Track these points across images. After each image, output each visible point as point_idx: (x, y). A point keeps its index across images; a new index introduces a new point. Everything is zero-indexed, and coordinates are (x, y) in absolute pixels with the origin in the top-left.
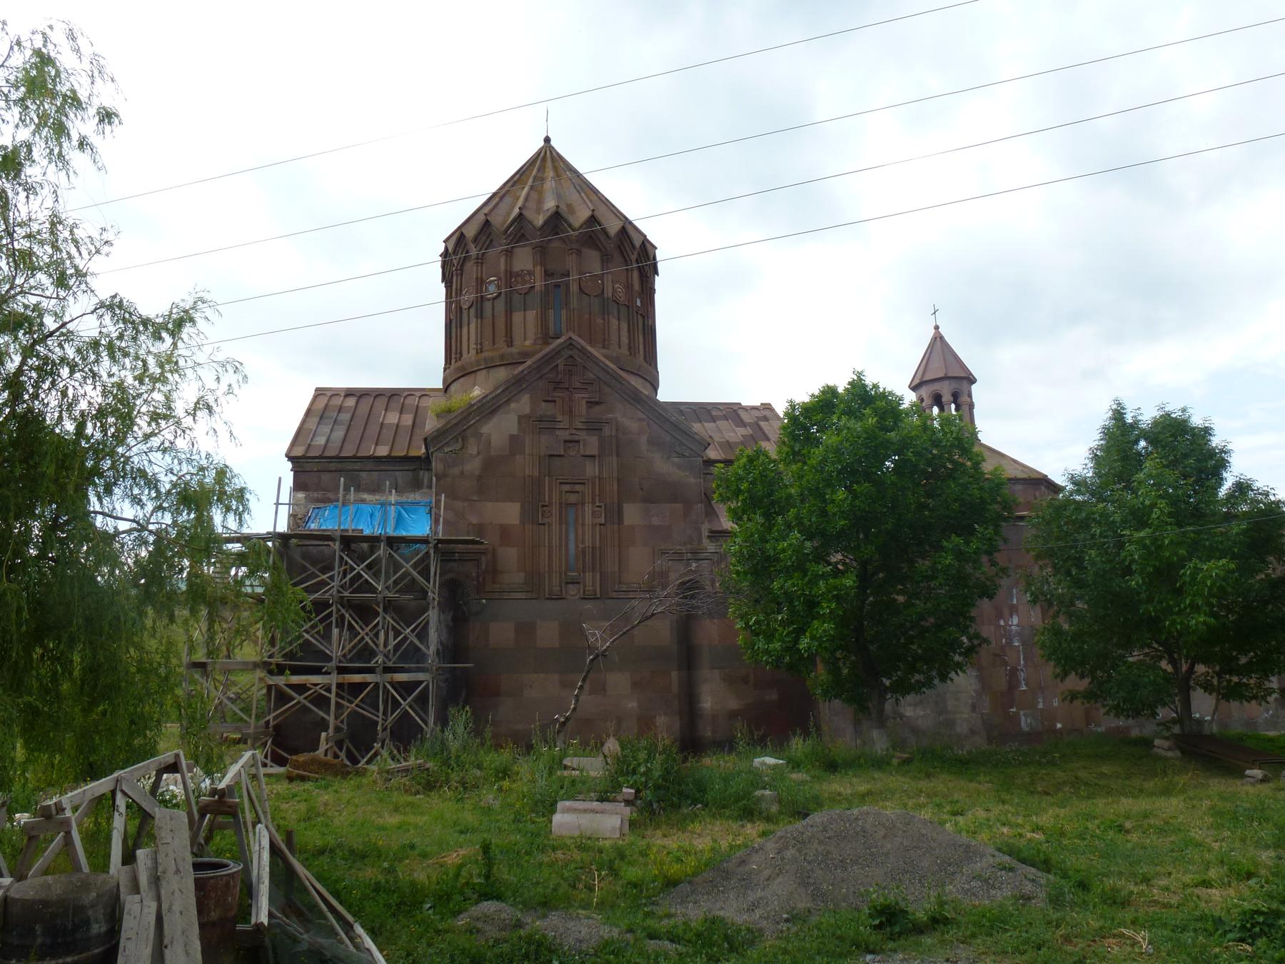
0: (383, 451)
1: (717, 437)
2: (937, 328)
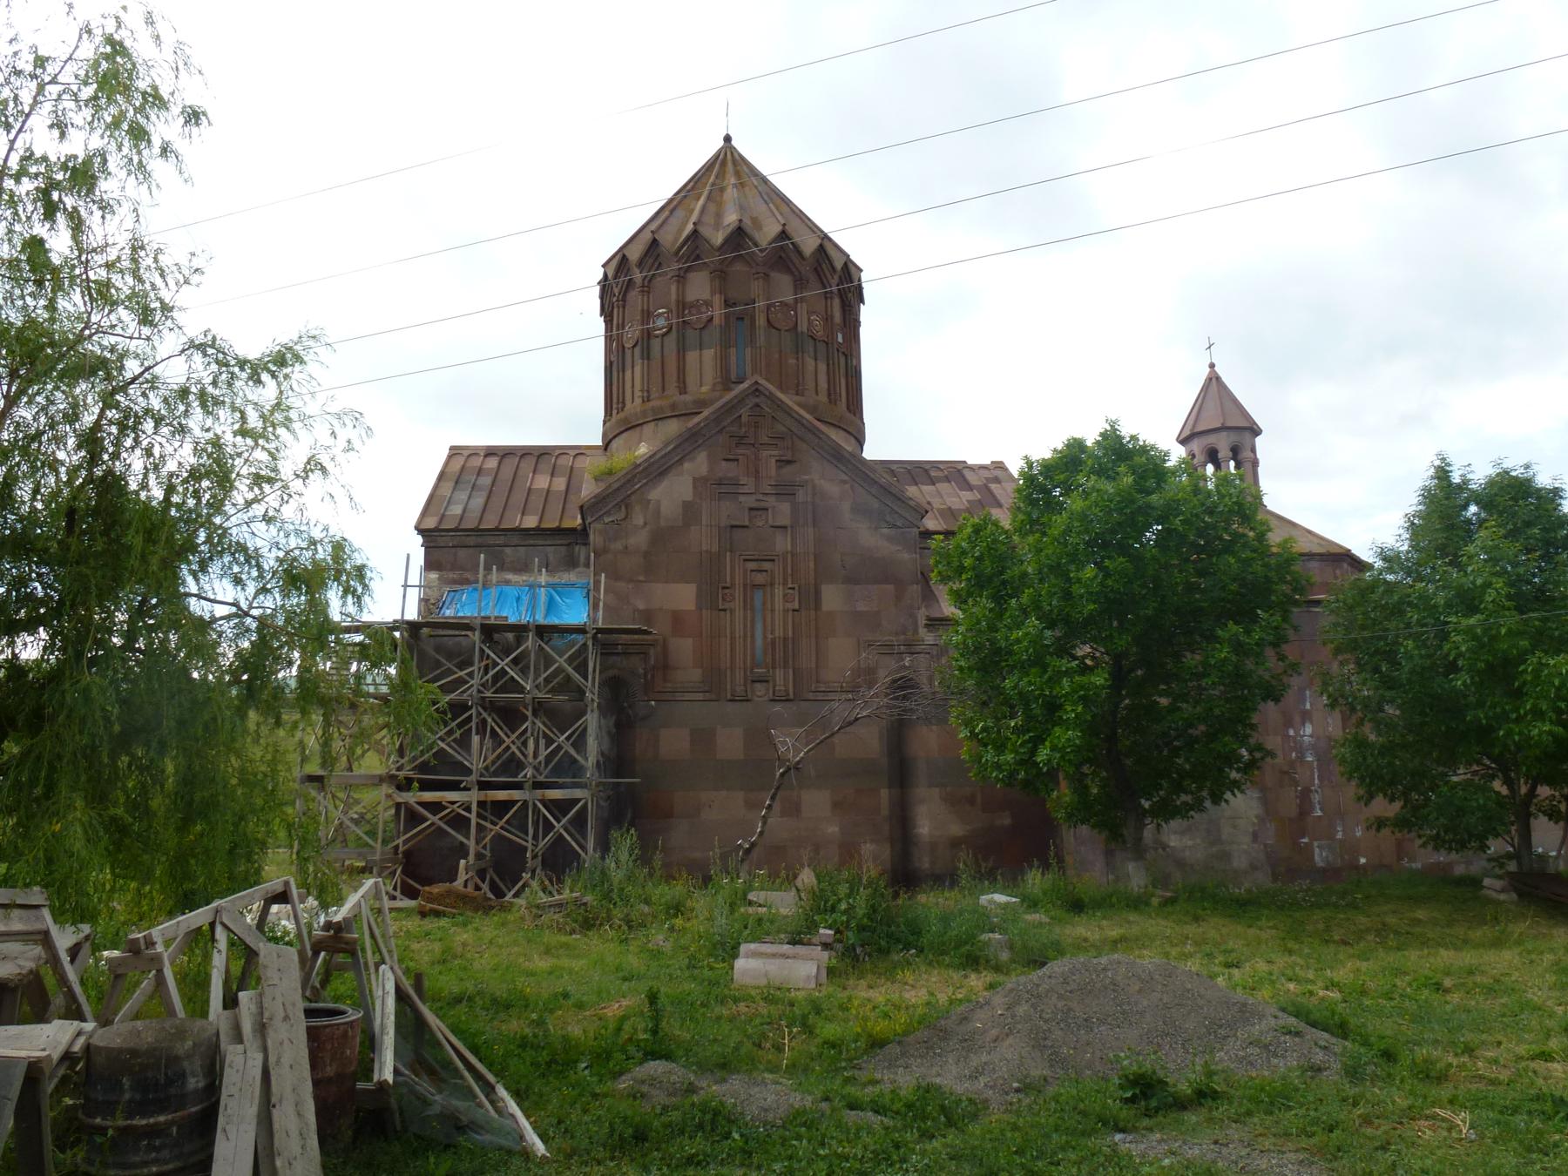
0: (531, 522)
1: (937, 503)
2: (1212, 366)
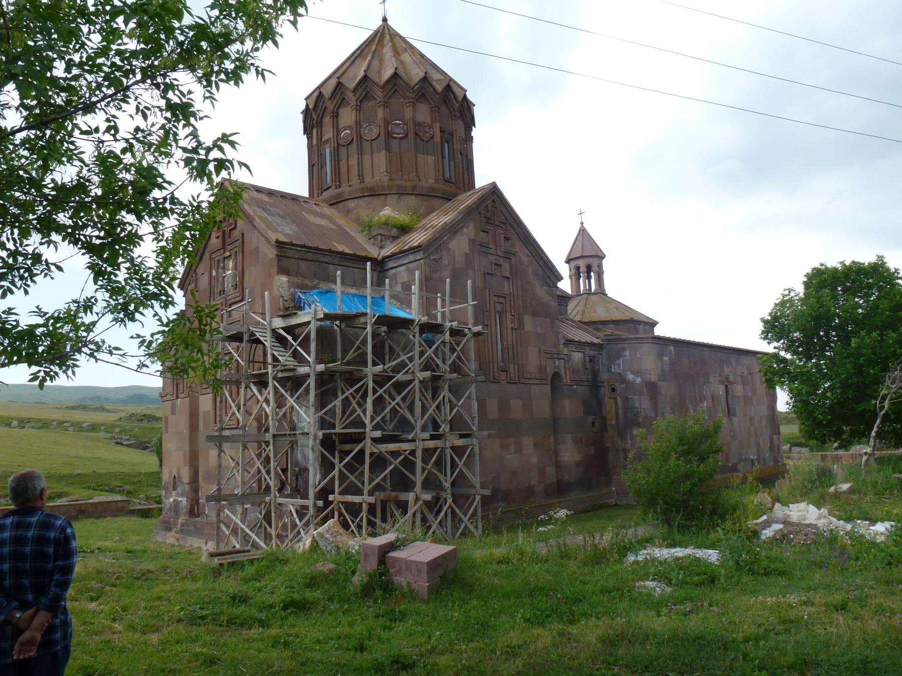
2: (582, 223)
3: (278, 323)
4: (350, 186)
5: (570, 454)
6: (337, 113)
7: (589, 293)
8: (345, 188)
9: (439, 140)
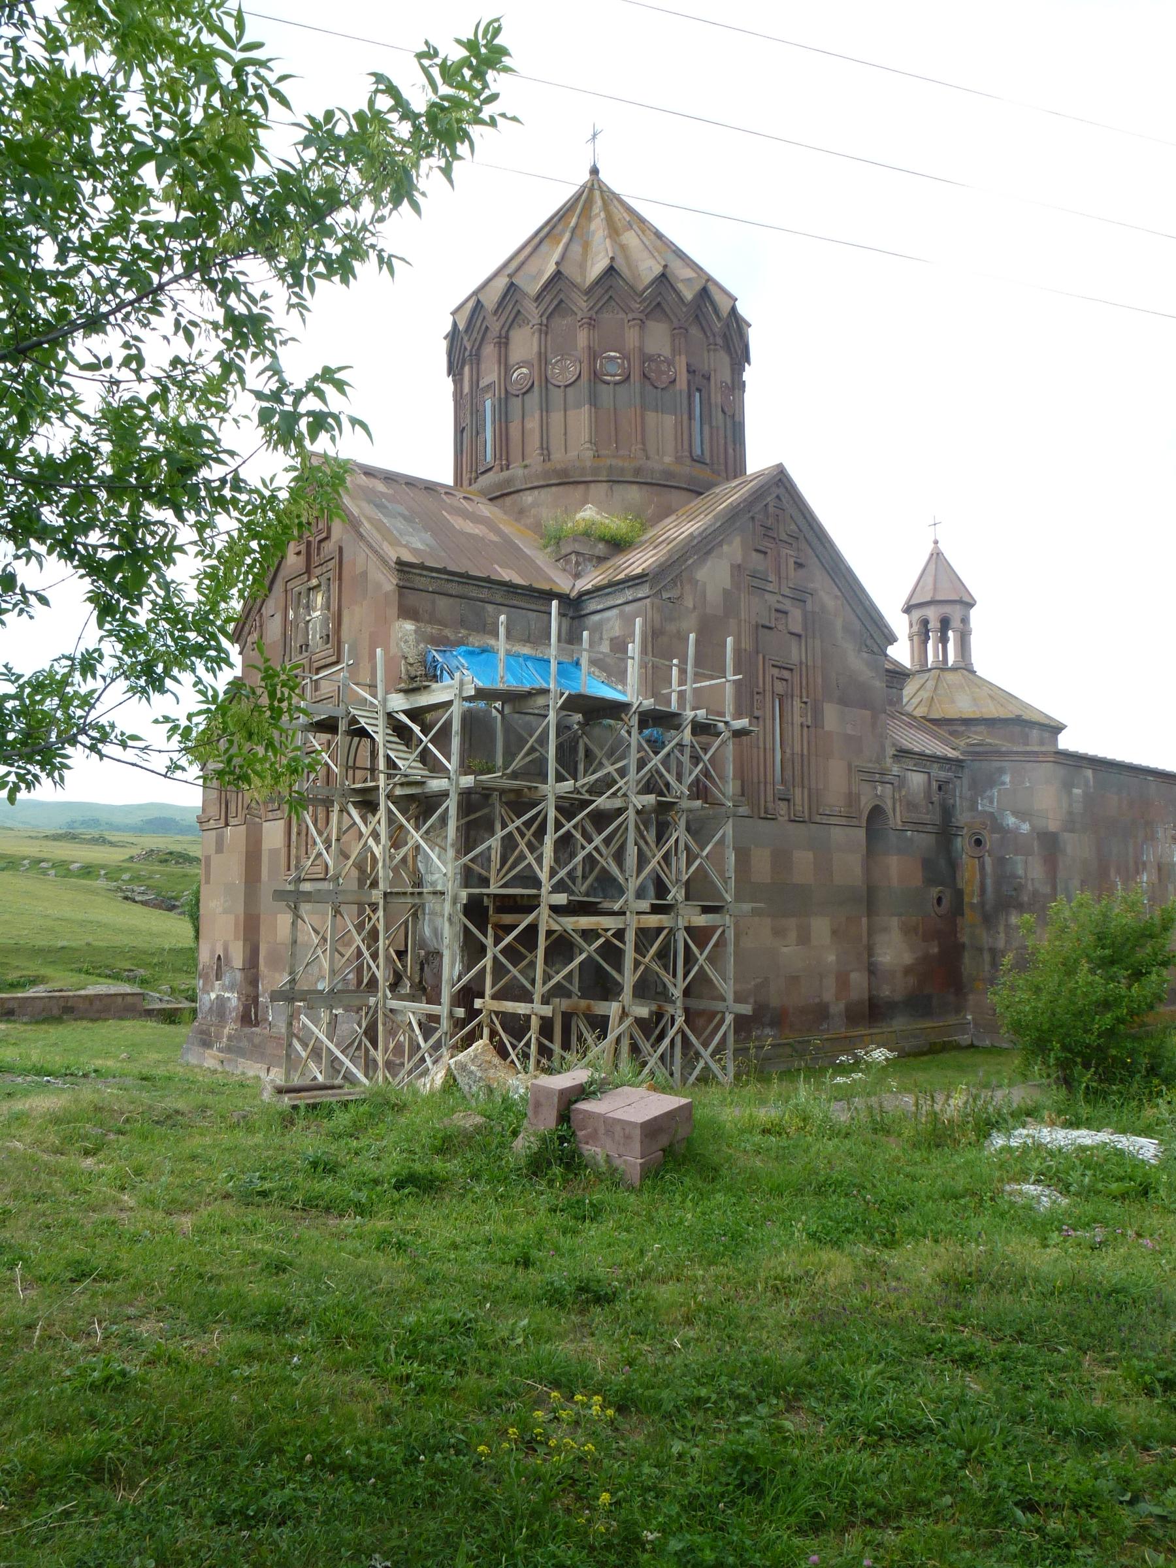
2: (936, 542)
3: (398, 703)
4: (526, 466)
5: (895, 952)
6: (507, 337)
7: (943, 667)
8: (517, 471)
9: (685, 387)
